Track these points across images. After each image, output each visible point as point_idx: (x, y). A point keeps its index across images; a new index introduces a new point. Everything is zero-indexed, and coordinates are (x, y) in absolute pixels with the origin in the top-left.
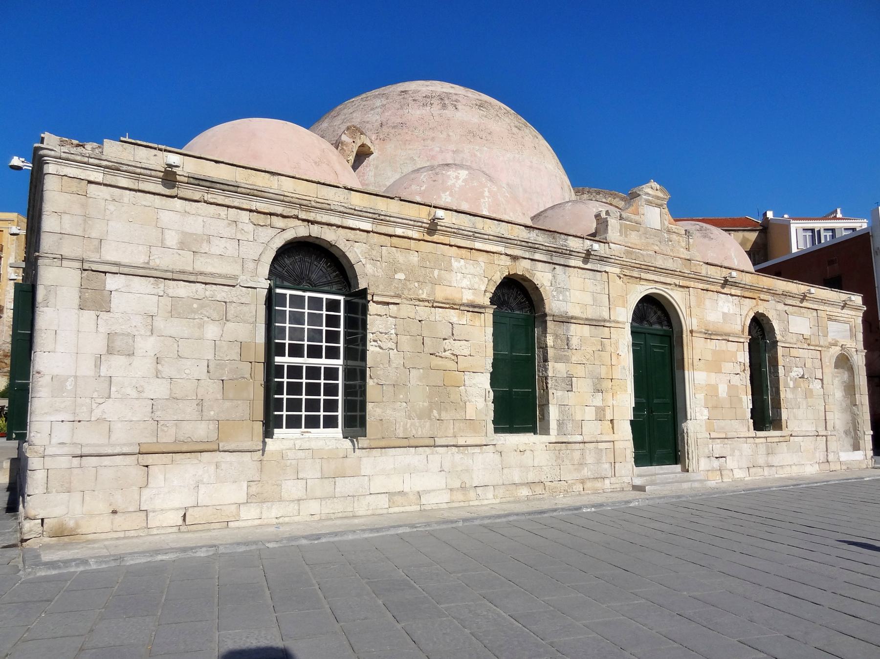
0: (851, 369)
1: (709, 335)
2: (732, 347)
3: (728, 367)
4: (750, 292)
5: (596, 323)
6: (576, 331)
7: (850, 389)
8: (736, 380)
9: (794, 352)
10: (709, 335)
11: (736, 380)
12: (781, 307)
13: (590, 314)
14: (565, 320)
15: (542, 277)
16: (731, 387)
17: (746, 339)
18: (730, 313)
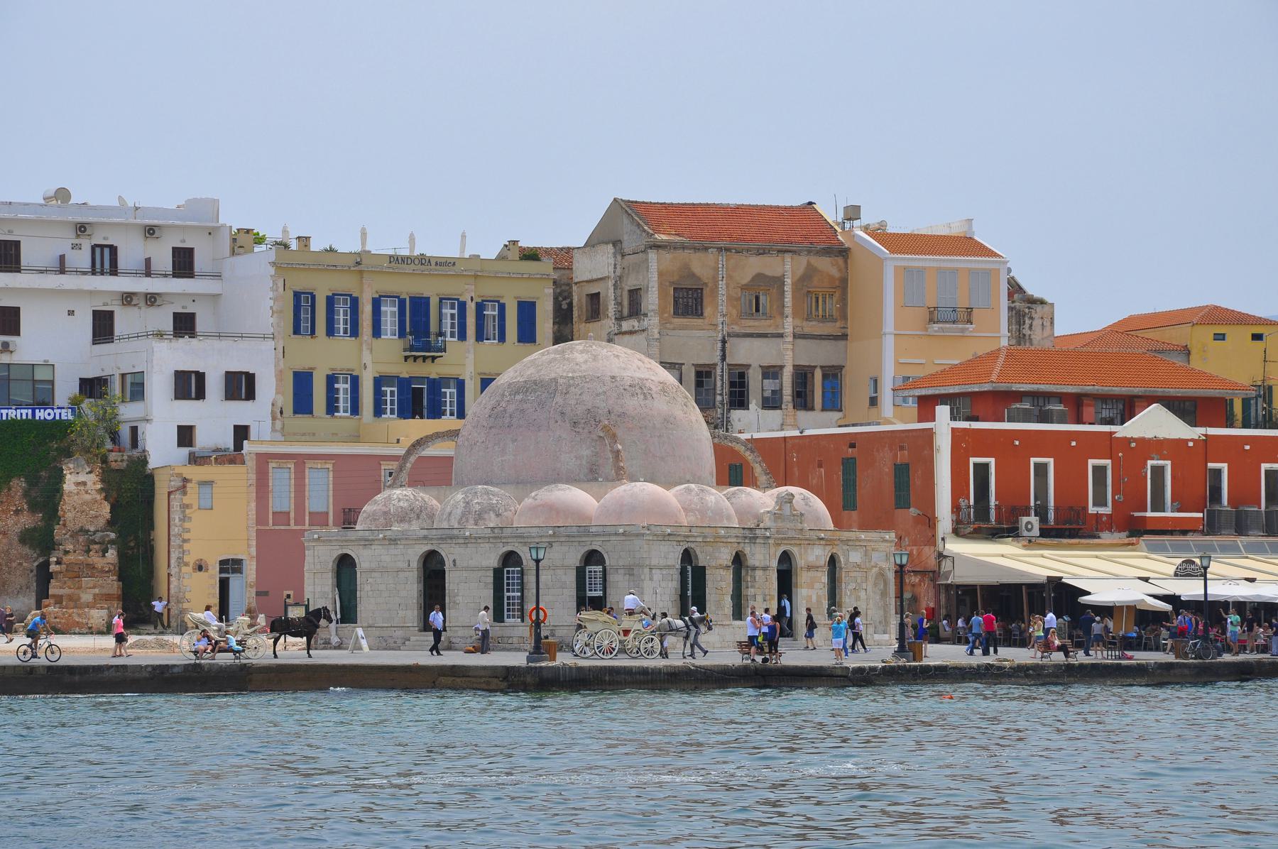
0: (886, 583)
1: (809, 568)
2: (819, 574)
3: (817, 585)
4: (829, 542)
5: (765, 569)
6: (759, 573)
7: (884, 594)
8: (820, 593)
9: (852, 574)
10: (809, 568)
11: (820, 593)
12: (845, 547)
13: (762, 565)
14: (754, 569)
15: (747, 550)
16: (819, 597)
17: (826, 569)
18: (819, 555)
